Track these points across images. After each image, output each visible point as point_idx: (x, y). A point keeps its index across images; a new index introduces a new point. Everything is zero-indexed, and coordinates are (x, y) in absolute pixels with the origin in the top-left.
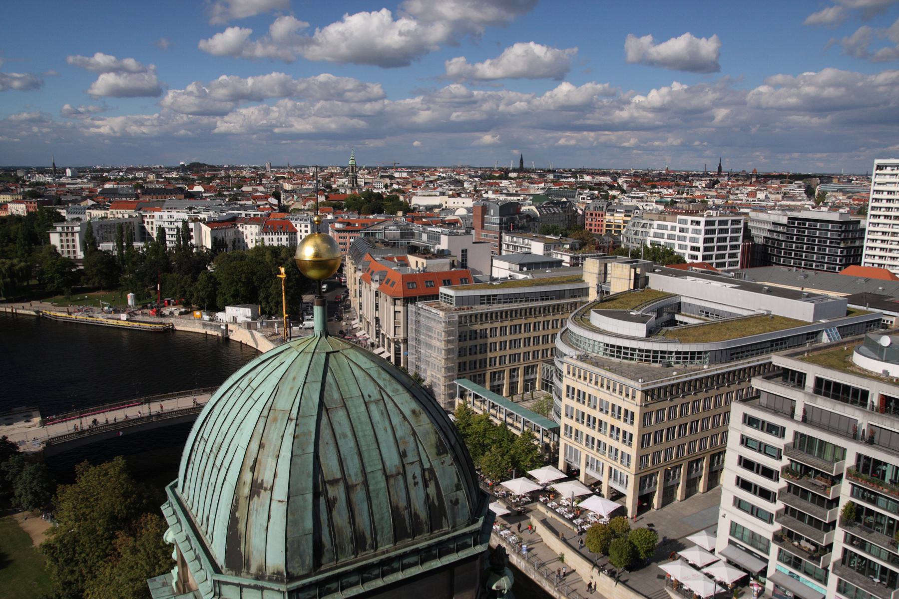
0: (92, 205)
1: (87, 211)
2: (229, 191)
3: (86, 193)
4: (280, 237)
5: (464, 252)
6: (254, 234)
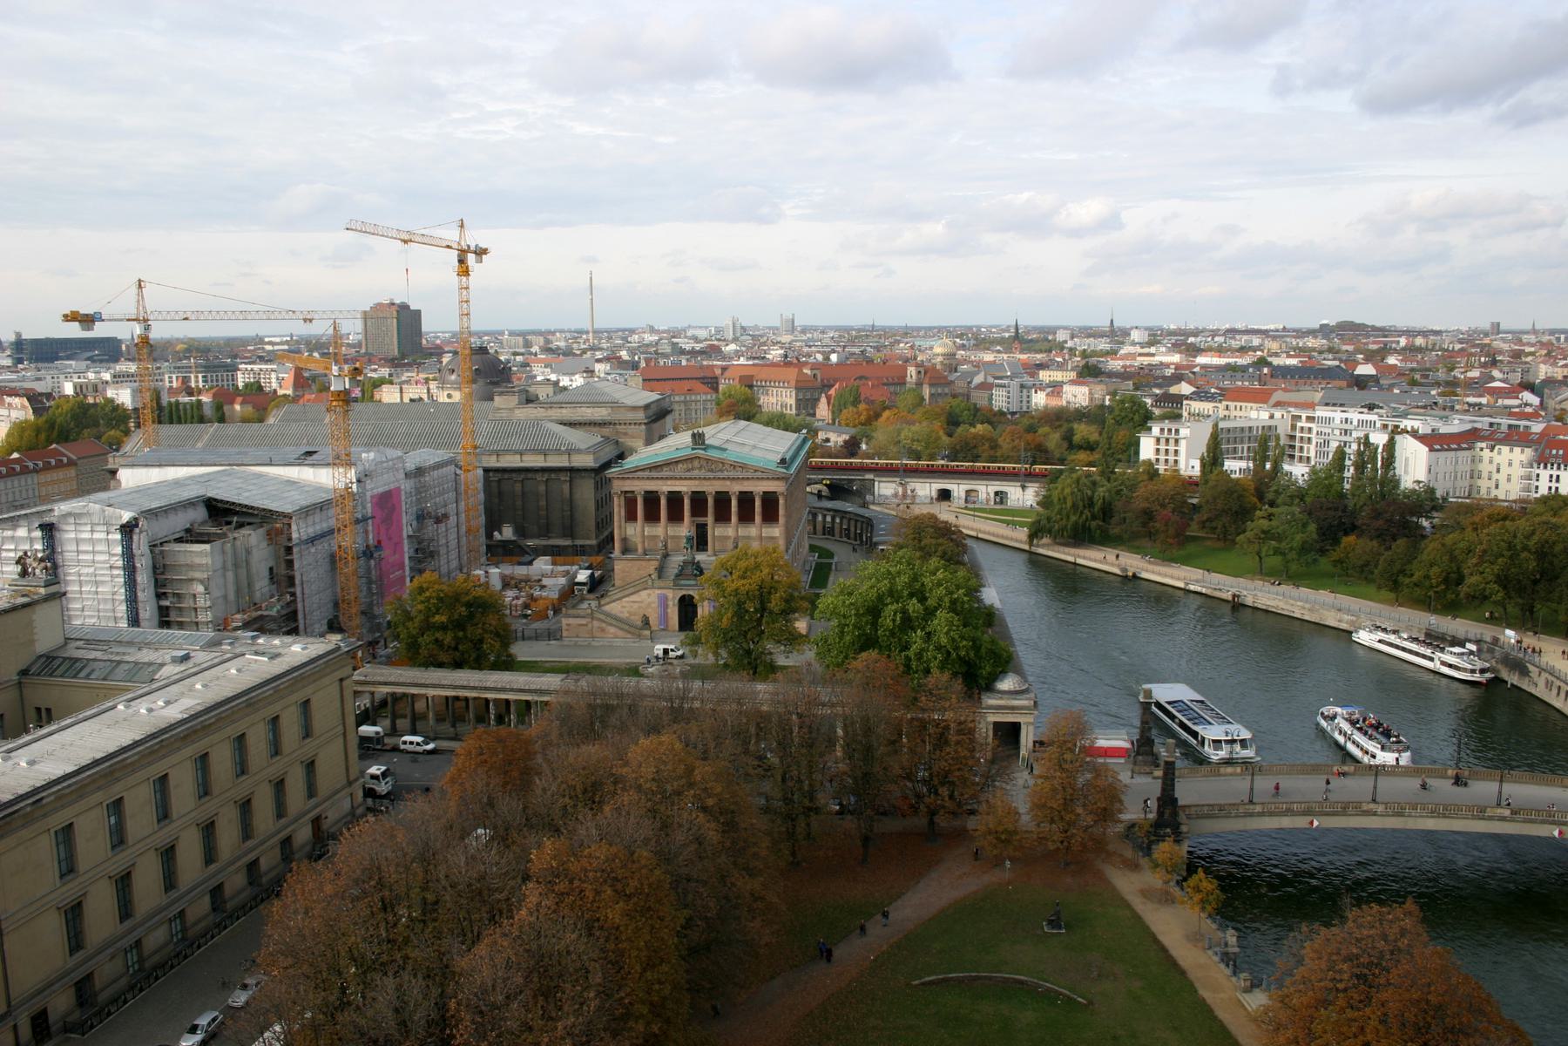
0: (1193, 393)
3: (1169, 372)
6: (1516, 464)
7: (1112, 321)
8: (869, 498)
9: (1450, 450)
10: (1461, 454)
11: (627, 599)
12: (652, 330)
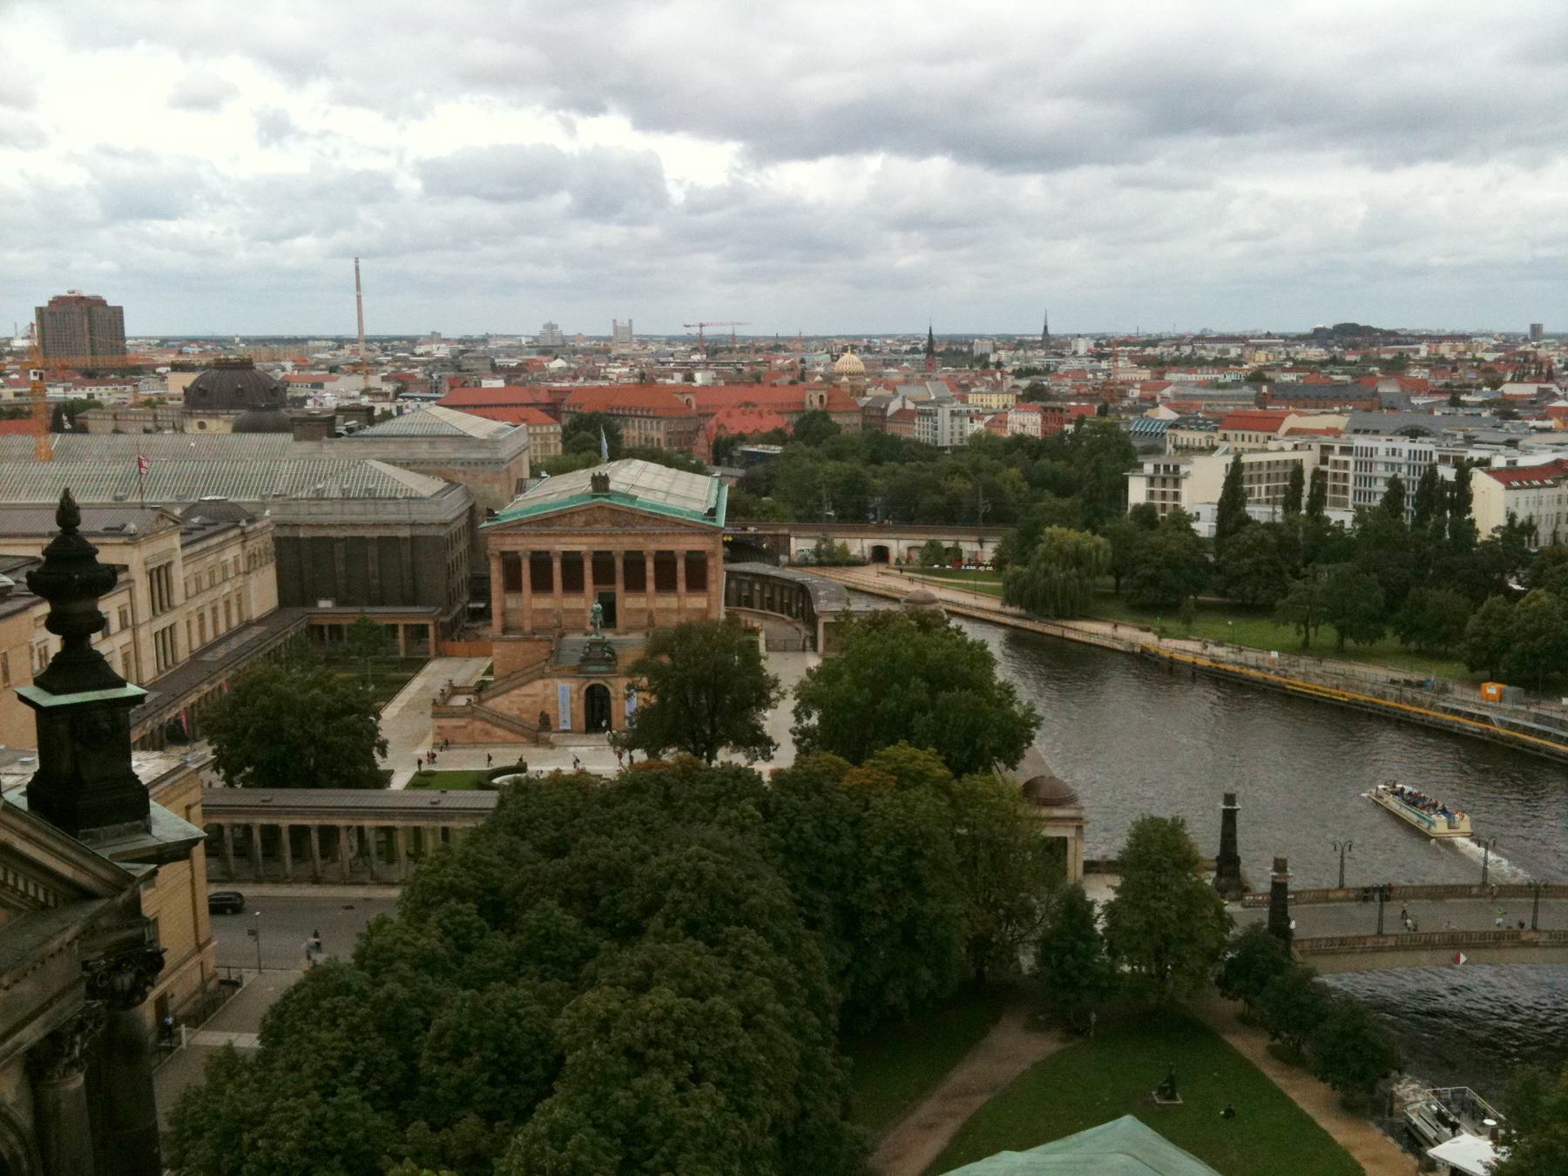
0: (1178, 420)
1: (1169, 431)
7: (1046, 328)
8: (784, 559)
9: (1532, 487)
10: (1545, 492)
11: (516, 692)
12: (435, 338)
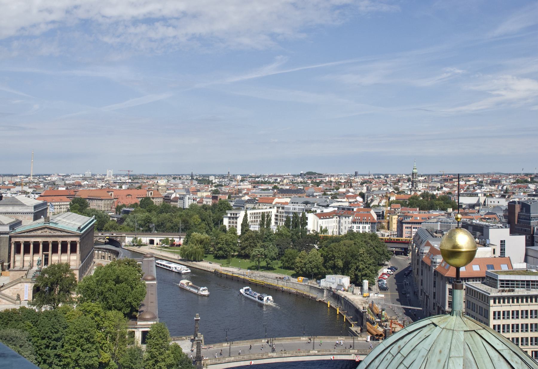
2: (331, 192)
4: (364, 225)
5: (503, 243)
6: (347, 223)
